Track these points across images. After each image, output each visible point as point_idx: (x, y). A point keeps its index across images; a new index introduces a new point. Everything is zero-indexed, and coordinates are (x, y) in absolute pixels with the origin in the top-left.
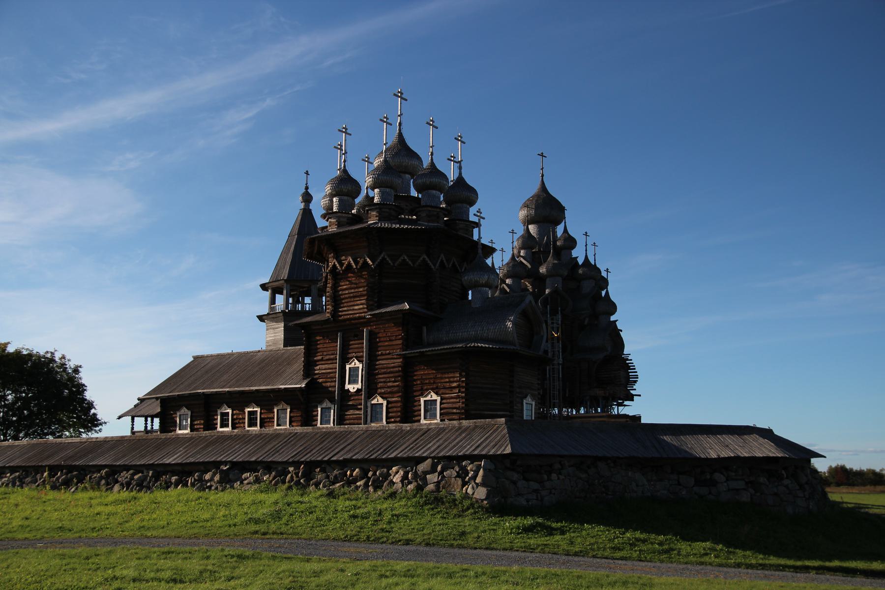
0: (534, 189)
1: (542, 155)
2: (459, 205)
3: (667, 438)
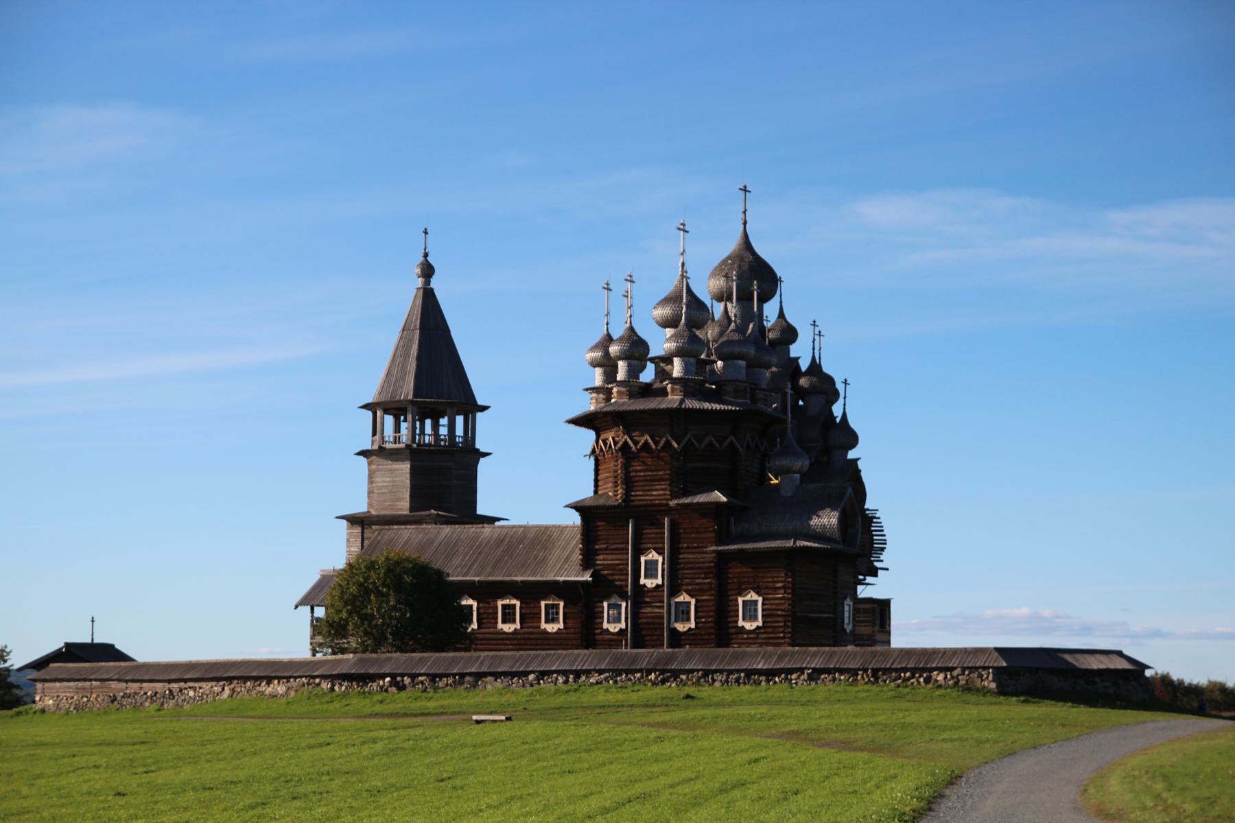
0: (730, 245)
1: (745, 190)
2: (757, 370)
3: (1067, 657)
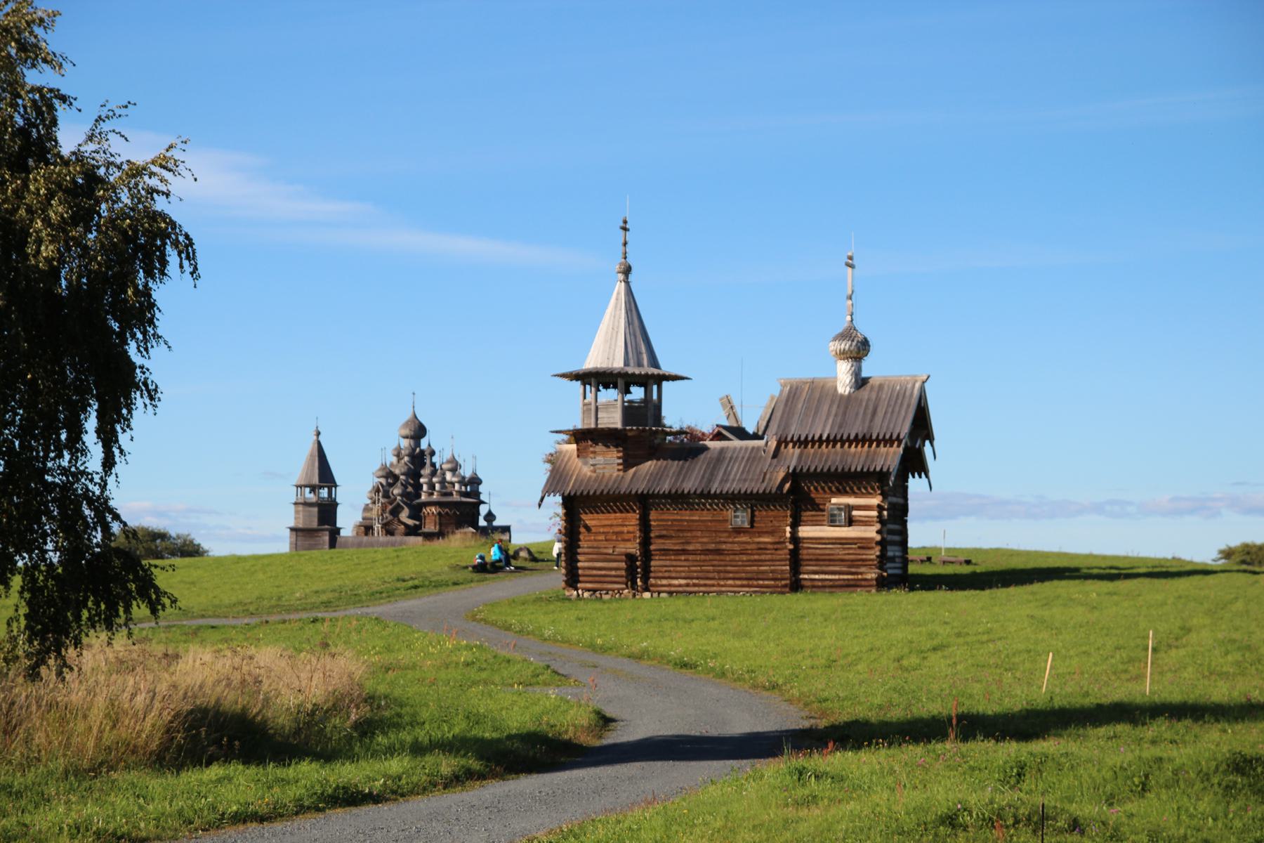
0: (409, 416)
